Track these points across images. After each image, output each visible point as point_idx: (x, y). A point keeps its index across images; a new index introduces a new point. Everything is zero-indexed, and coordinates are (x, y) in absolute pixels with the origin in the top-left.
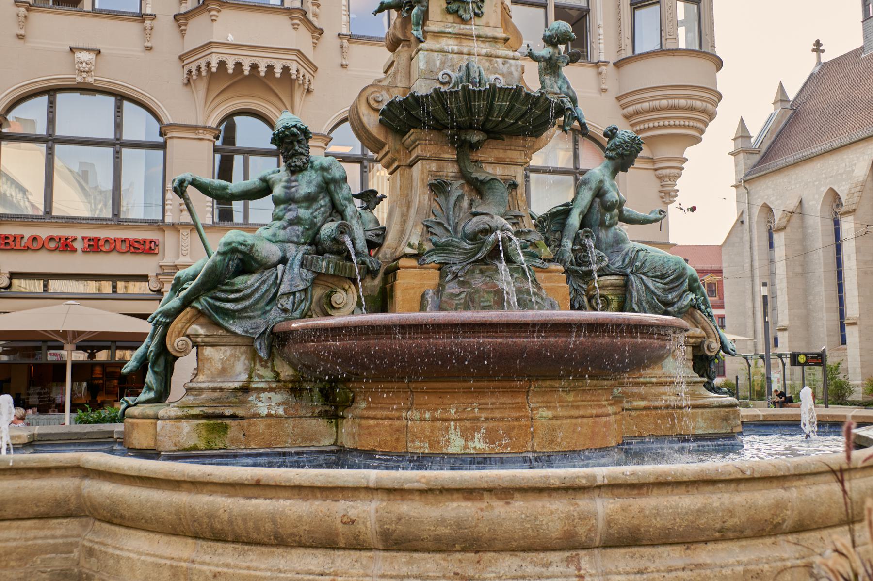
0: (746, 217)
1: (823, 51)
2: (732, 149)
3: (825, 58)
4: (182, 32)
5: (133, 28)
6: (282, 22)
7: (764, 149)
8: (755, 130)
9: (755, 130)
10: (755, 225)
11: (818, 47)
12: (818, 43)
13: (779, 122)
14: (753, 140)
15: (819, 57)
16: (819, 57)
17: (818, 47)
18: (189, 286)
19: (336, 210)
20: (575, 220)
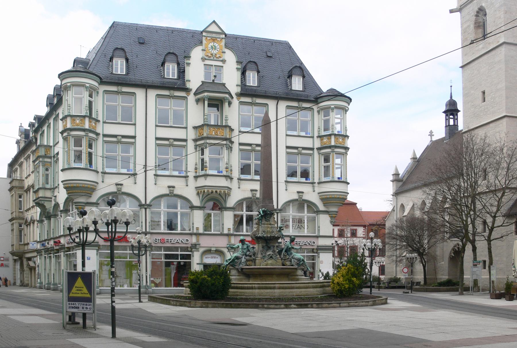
0: (395, 209)
1: (433, 135)
2: (392, 179)
3: (434, 139)
4: (196, 181)
5: (184, 179)
6: (224, 179)
7: (405, 179)
8: (401, 172)
9: (401, 172)
10: (398, 212)
11: (431, 134)
12: (431, 132)
13: (412, 167)
14: (400, 175)
15: (431, 138)
16: (431, 138)
17: (431, 134)
18: (229, 261)
19: (249, 251)
20: (284, 251)
